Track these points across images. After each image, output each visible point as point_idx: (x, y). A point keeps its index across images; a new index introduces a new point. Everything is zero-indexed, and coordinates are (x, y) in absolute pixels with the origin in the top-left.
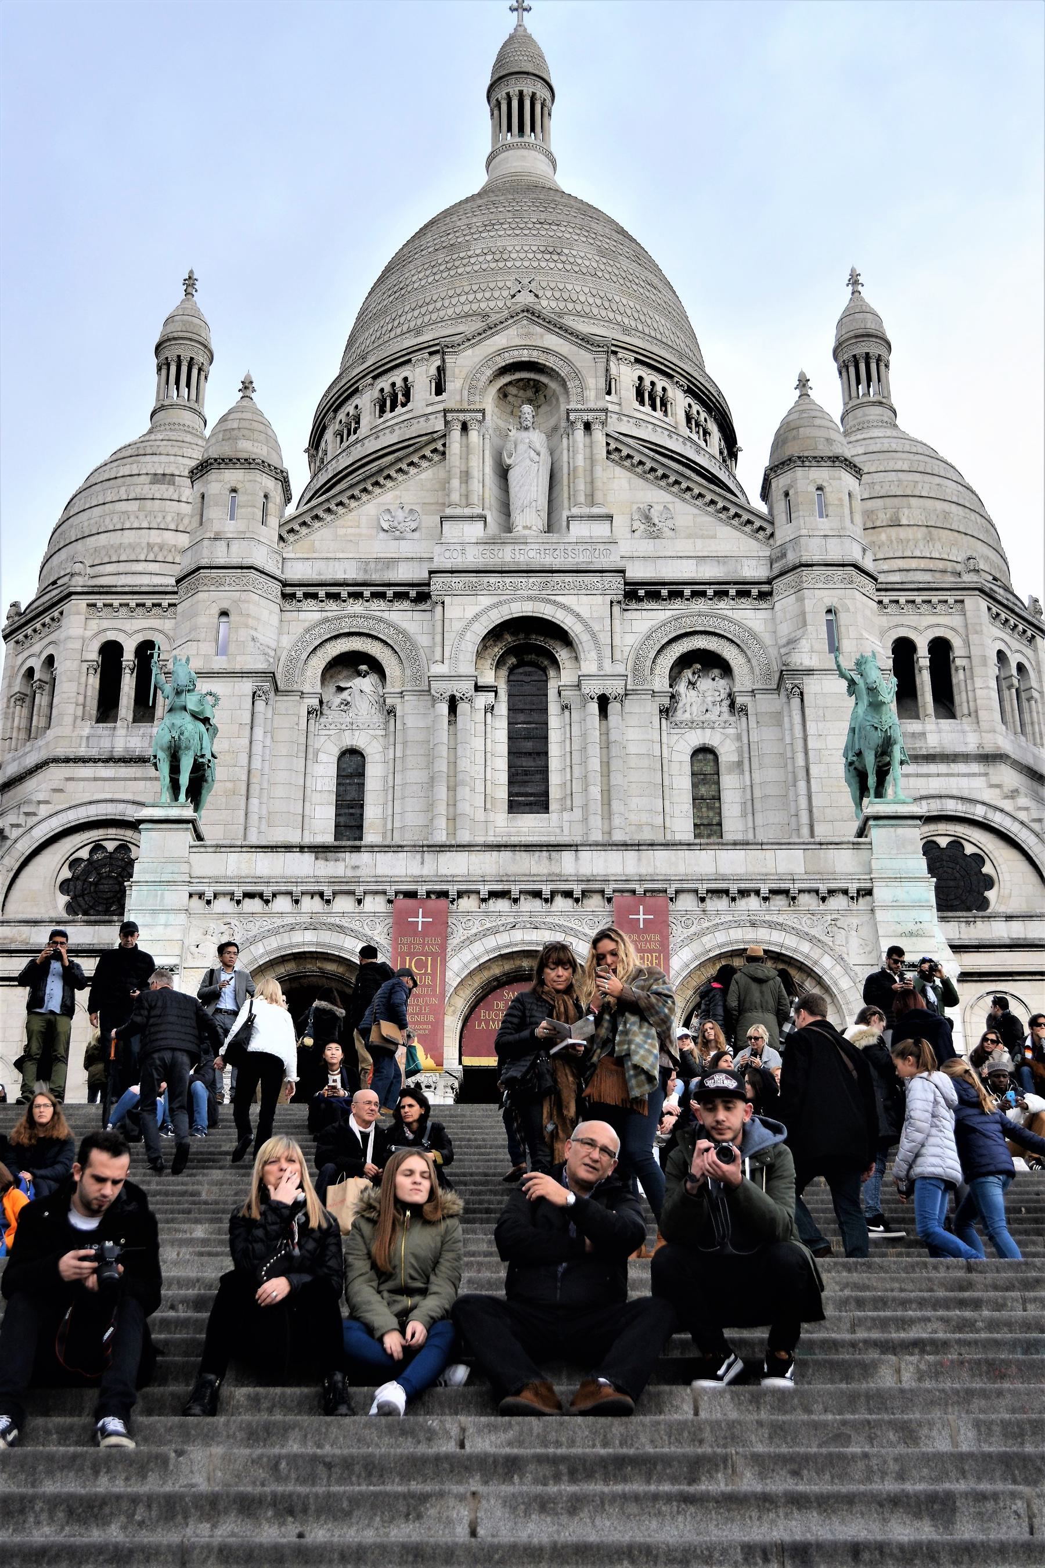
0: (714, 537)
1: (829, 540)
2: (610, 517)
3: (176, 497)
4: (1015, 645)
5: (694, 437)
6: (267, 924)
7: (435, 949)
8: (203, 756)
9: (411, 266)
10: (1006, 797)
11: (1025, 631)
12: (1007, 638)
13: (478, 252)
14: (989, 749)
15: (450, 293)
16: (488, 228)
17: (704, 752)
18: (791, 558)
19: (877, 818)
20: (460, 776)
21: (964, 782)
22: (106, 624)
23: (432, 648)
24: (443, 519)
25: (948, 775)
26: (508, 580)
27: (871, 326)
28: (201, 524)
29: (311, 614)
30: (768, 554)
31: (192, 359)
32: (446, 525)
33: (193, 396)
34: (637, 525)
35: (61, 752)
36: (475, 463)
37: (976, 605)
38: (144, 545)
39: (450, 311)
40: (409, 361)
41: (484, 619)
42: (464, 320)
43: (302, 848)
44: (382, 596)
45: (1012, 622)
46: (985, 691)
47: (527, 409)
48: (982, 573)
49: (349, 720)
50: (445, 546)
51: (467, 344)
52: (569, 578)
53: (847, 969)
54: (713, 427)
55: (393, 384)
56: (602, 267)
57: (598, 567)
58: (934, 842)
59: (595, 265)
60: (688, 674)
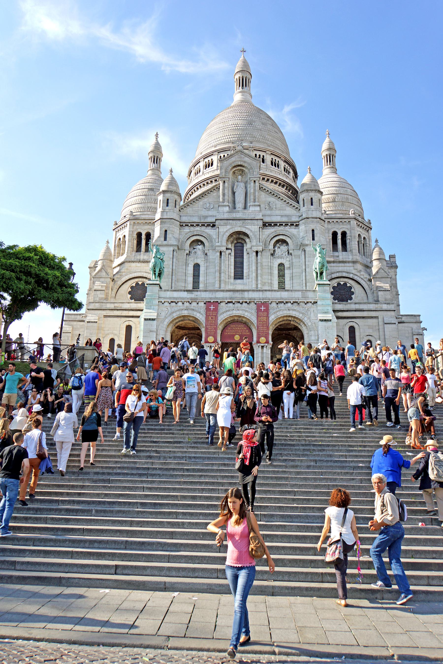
0: (285, 210)
2: (260, 206)
5: (286, 174)
6: (176, 309)
7: (215, 314)
10: (358, 272)
12: (361, 230)
14: (354, 260)
18: (304, 216)
19: (319, 285)
21: (348, 268)
22: (138, 227)
24: (219, 206)
25: (344, 266)
26: (234, 222)
27: (331, 147)
28: (160, 207)
29: (187, 229)
33: (158, 167)
35: (128, 260)
36: (226, 191)
37: (354, 222)
39: (223, 141)
41: (228, 232)
43: (184, 291)
44: (204, 225)
47: (240, 177)
52: (249, 221)
57: (256, 218)
60: (278, 245)
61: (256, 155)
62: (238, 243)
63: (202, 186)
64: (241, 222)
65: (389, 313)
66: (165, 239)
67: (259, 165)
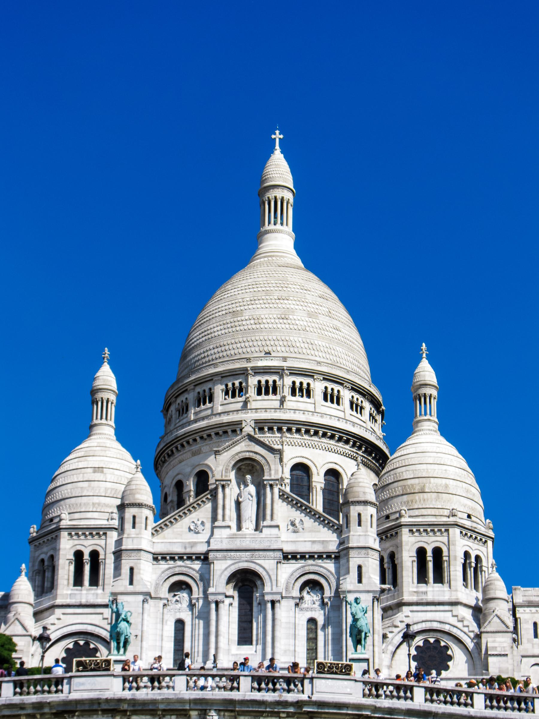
0: (319, 532)
1: (361, 537)
2: (278, 526)
3: (104, 480)
5: (354, 413)
8: (127, 635)
9: (214, 321)
10: (459, 621)
11: (481, 540)
13: (247, 318)
14: (453, 599)
15: (233, 341)
16: (253, 302)
17: (312, 621)
20: (220, 633)
21: (442, 614)
22: (77, 542)
23: (209, 579)
26: (238, 554)
29: (163, 565)
31: (108, 399)
32: (216, 530)
34: (290, 527)
35: (59, 601)
37: (455, 532)
38: (91, 504)
40: (212, 380)
42: (238, 361)
45: (474, 536)
46: (455, 572)
47: (248, 477)
49: (178, 608)
50: (215, 539)
51: (224, 450)
52: (261, 553)
55: (204, 391)
56: (309, 324)
57: (272, 548)
58: (429, 641)
59: (305, 323)
60: (307, 588)
61: (294, 383)
62: (243, 585)
63: (191, 441)
64: (248, 553)
66: (131, 583)
67: (278, 456)
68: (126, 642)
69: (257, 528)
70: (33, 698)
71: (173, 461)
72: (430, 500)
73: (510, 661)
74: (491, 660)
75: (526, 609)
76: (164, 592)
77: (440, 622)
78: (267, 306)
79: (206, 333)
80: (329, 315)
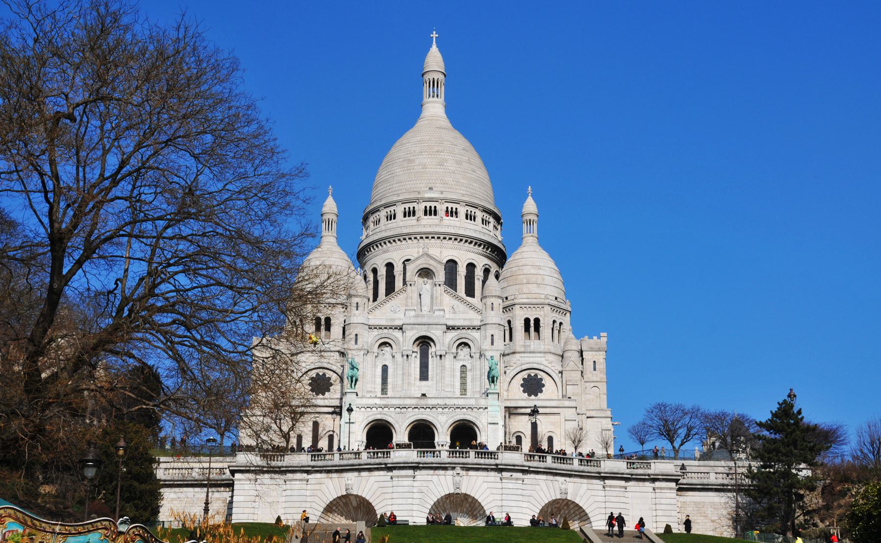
0: (468, 313)
4: (560, 317)
5: (484, 226)
6: (371, 413)
12: (557, 316)
15: (408, 179)
21: (539, 359)
24: (406, 310)
26: (420, 326)
29: (376, 332)
30: (480, 318)
37: (547, 308)
39: (408, 186)
48: (551, 298)
52: (434, 326)
53: (482, 424)
54: (492, 220)
55: (391, 211)
60: (460, 347)
61: (447, 208)
63: (383, 244)
64: (426, 326)
65: (571, 410)
68: (356, 380)
69: (432, 310)
70: (378, 461)
71: (369, 255)
72: (533, 288)
73: (580, 389)
74: (568, 387)
75: (589, 352)
76: (375, 348)
77: (538, 364)
78: (430, 156)
79: (390, 173)
80: (469, 162)
